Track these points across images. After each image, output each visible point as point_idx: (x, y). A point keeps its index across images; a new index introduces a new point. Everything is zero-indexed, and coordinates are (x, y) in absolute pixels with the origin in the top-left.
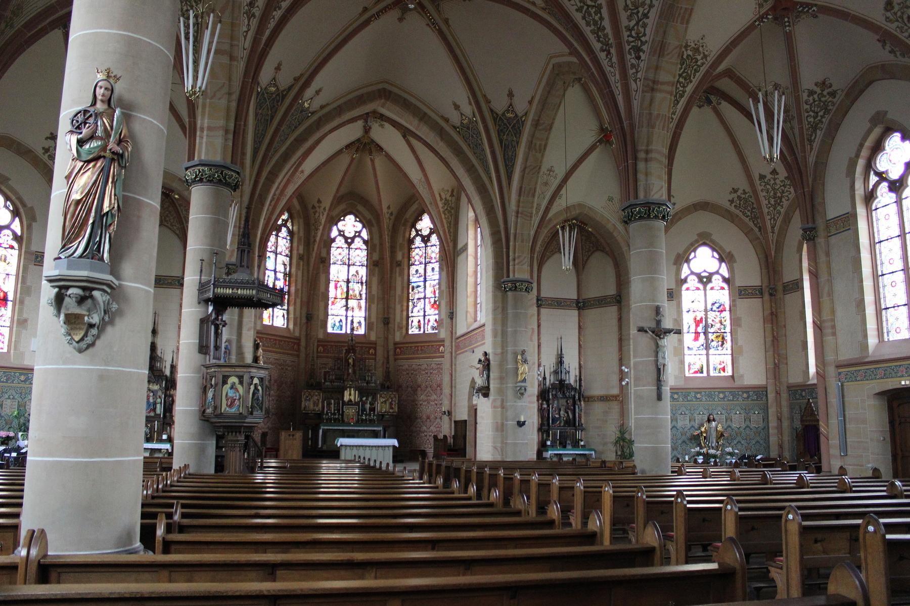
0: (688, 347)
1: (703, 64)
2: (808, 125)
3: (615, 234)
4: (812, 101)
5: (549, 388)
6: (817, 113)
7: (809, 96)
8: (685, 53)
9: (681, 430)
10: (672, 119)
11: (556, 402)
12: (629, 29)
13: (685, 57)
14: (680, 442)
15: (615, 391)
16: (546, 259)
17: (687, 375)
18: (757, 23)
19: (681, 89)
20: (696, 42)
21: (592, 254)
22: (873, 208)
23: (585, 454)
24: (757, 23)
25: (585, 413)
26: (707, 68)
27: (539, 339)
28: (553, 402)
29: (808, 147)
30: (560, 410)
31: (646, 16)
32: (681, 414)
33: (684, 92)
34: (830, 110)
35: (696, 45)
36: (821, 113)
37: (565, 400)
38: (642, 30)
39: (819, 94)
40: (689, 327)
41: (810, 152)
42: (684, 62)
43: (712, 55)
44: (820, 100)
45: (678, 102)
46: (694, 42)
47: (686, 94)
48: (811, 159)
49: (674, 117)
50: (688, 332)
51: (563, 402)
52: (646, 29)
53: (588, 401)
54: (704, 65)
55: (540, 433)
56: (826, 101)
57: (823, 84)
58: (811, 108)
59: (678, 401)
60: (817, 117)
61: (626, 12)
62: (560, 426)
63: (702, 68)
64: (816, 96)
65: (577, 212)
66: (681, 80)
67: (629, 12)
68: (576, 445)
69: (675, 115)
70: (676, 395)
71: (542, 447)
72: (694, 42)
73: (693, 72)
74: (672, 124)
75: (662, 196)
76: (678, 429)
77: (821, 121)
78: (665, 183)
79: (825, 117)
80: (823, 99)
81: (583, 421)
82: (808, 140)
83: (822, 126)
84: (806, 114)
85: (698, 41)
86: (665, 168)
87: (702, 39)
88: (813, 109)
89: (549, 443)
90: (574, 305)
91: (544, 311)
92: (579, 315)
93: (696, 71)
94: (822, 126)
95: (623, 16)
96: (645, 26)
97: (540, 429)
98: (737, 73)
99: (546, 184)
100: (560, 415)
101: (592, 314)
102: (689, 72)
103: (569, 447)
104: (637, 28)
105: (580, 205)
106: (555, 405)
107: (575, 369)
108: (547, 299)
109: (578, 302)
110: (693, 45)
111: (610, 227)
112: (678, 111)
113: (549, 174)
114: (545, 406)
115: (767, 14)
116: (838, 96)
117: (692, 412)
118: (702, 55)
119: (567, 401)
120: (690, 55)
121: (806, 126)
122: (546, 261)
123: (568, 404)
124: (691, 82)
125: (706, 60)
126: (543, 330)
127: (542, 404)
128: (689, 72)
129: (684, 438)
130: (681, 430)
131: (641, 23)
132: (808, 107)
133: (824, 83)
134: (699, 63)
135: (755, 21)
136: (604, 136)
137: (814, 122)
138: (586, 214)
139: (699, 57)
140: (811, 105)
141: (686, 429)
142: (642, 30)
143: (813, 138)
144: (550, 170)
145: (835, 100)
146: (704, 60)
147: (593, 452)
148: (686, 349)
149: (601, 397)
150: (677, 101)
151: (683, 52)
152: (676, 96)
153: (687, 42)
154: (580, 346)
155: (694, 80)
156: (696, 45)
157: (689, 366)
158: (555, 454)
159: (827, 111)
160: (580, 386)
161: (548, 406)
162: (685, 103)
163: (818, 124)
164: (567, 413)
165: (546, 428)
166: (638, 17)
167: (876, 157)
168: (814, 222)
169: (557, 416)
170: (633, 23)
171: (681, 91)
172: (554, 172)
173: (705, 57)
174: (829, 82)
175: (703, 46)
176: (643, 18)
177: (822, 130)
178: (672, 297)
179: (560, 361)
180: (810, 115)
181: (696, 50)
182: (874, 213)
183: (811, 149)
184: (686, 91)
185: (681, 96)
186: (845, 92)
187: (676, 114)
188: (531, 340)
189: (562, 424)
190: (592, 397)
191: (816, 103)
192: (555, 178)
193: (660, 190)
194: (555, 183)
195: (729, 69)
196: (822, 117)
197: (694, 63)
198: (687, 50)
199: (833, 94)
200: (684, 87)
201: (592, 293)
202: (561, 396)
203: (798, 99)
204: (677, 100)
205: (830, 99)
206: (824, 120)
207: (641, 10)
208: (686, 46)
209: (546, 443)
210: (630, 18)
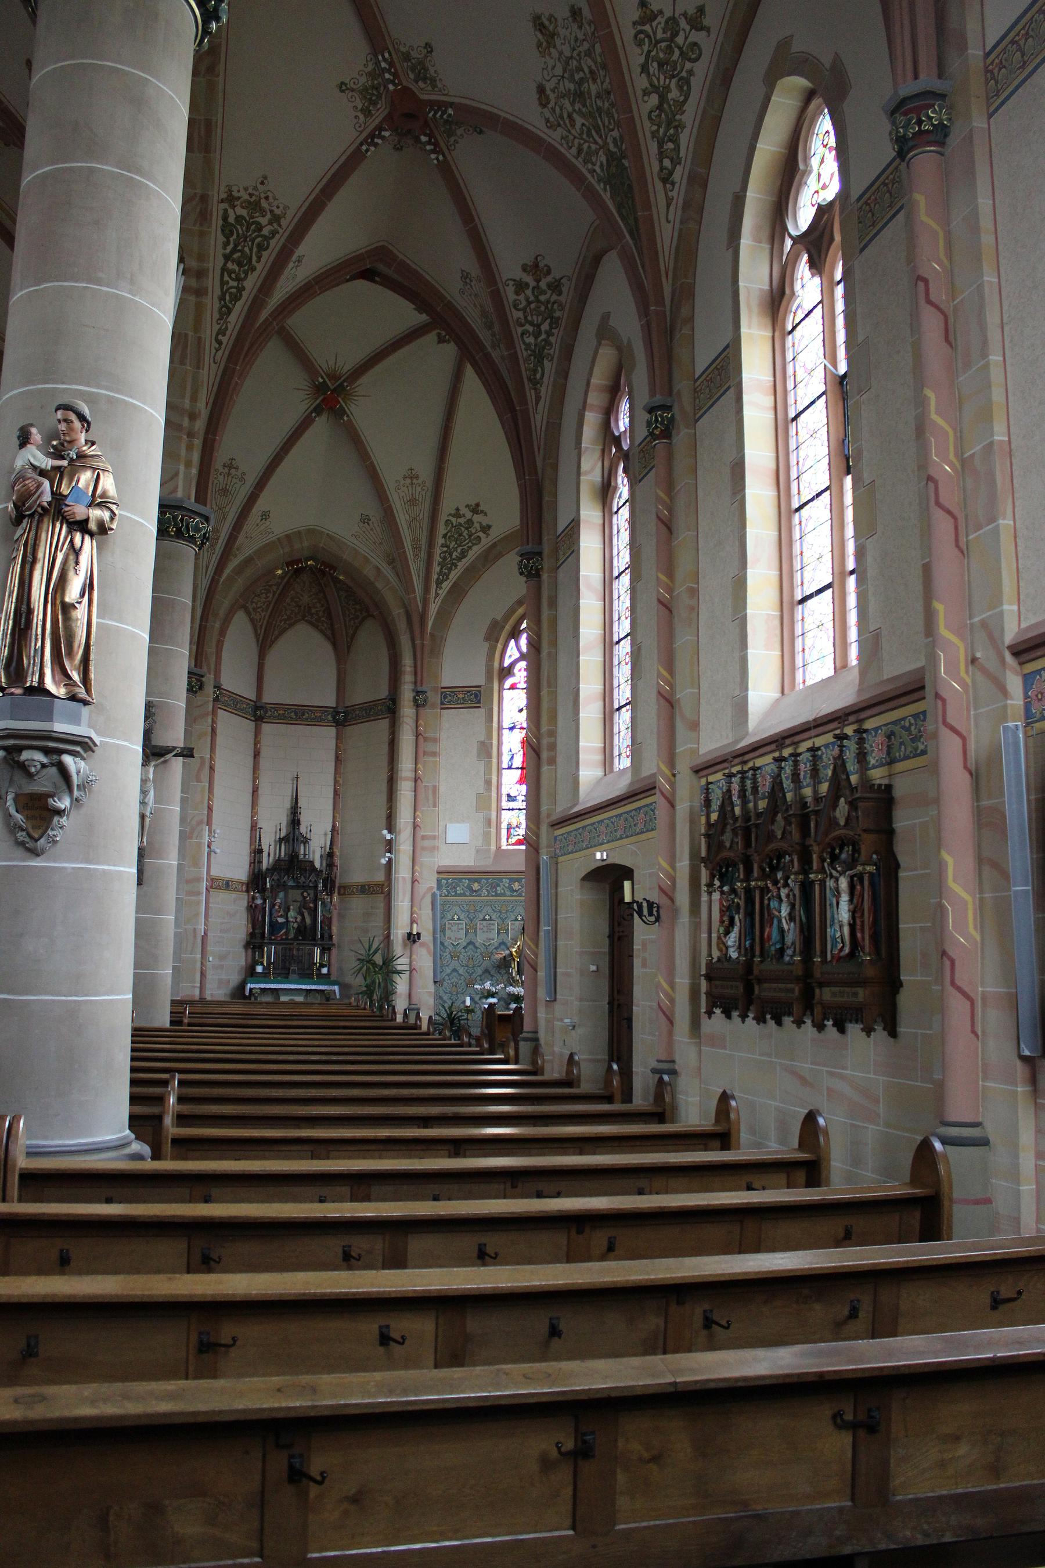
0: (509, 795)
1: (274, 233)
2: (526, 350)
3: (379, 585)
4: (524, 303)
5: (267, 869)
6: (539, 326)
7: (517, 293)
8: (230, 211)
9: (483, 949)
10: (220, 343)
11: (281, 895)
13: (231, 219)
14: (479, 971)
15: (380, 877)
16: (276, 632)
17: (504, 847)
18: (364, 148)
19: (235, 284)
20: (250, 191)
21: (361, 623)
22: (615, 509)
23: (322, 991)
24: (364, 148)
25: (339, 914)
26: (283, 240)
27: (255, 778)
29: (530, 394)
30: (289, 910)
32: (484, 919)
33: (241, 290)
34: (559, 318)
35: (251, 195)
36: (545, 327)
37: (299, 891)
39: (534, 288)
40: (512, 757)
41: (537, 404)
42: (232, 234)
43: (289, 216)
44: (538, 301)
45: (230, 311)
46: (246, 189)
47: (245, 294)
48: (538, 417)
49: (224, 339)
50: (510, 768)
51: (295, 894)
53: (344, 894)
54: (277, 236)
55: (250, 951)
56: (548, 302)
57: (535, 268)
58: (526, 317)
59: (480, 896)
60: (540, 333)
63: (273, 242)
64: (529, 292)
65: (306, 544)
66: (230, 265)
68: (307, 973)
69: (224, 335)
70: (476, 884)
71: (250, 973)
72: (246, 189)
73: (255, 249)
74: (220, 353)
75: (175, 490)
76: (476, 948)
77: (547, 342)
78: (188, 464)
79: (553, 335)
80: (542, 298)
81: (335, 929)
82: (529, 379)
83: (551, 352)
84: (520, 330)
85: (255, 188)
86: (191, 435)
87: (262, 183)
88: (529, 318)
89: (259, 969)
90: (330, 718)
91: (266, 728)
92: (339, 737)
93: (261, 248)
94: (551, 352)
97: (247, 946)
98: (398, 254)
99: (225, 491)
100: (287, 918)
101: (356, 732)
102: (247, 249)
103: (292, 976)
105: (311, 532)
106: (279, 901)
107: (326, 834)
108: (276, 706)
109: (335, 711)
110: (246, 197)
111: (369, 572)
112: (230, 327)
113: (229, 474)
114: (259, 902)
115: (380, 128)
116: (564, 289)
117: (503, 916)
118: (269, 216)
119: (302, 894)
120: (243, 217)
121: (523, 353)
122: (277, 638)
124: (253, 269)
125: (280, 226)
126: (263, 762)
127: (254, 898)
128: (247, 249)
129: (487, 964)
130: (483, 949)
132: (520, 314)
133: (536, 265)
134: (265, 232)
135: (361, 144)
136: (323, 401)
137: (536, 345)
138: (323, 549)
139: (264, 221)
140: (524, 310)
141: (491, 949)
143: (538, 376)
144: (230, 466)
145: (562, 299)
146: (275, 225)
147: (336, 988)
148: (504, 798)
149: (361, 886)
150: (228, 308)
151: (226, 211)
152: (222, 298)
153: (230, 191)
154: (336, 793)
155: (259, 267)
156: (251, 195)
157: (508, 830)
158: (261, 989)
159: (555, 322)
160: (331, 865)
161: (264, 902)
162: (244, 314)
163: (544, 348)
165: (258, 941)
167: (618, 407)
168: (540, 543)
169: (281, 920)
171: (232, 287)
172: (237, 469)
173: (276, 219)
174: (545, 262)
175: (267, 198)
177: (552, 360)
178: (479, 702)
179: (295, 822)
180: (528, 331)
181: (254, 206)
182: (615, 517)
183: (538, 399)
184: (244, 289)
185: (236, 298)
186: (574, 281)
187: (228, 333)
188: (199, 780)
189: (291, 936)
190: (350, 886)
191: (533, 306)
192: (242, 479)
193: (172, 478)
194: (243, 492)
195: (383, 247)
196: (549, 334)
197: (255, 231)
198: (233, 207)
199: (556, 287)
200: (238, 279)
201: (361, 694)
202: (291, 883)
203: (497, 296)
204: (226, 306)
205: (554, 297)
206: (552, 339)
208: (231, 199)
209: (255, 969)
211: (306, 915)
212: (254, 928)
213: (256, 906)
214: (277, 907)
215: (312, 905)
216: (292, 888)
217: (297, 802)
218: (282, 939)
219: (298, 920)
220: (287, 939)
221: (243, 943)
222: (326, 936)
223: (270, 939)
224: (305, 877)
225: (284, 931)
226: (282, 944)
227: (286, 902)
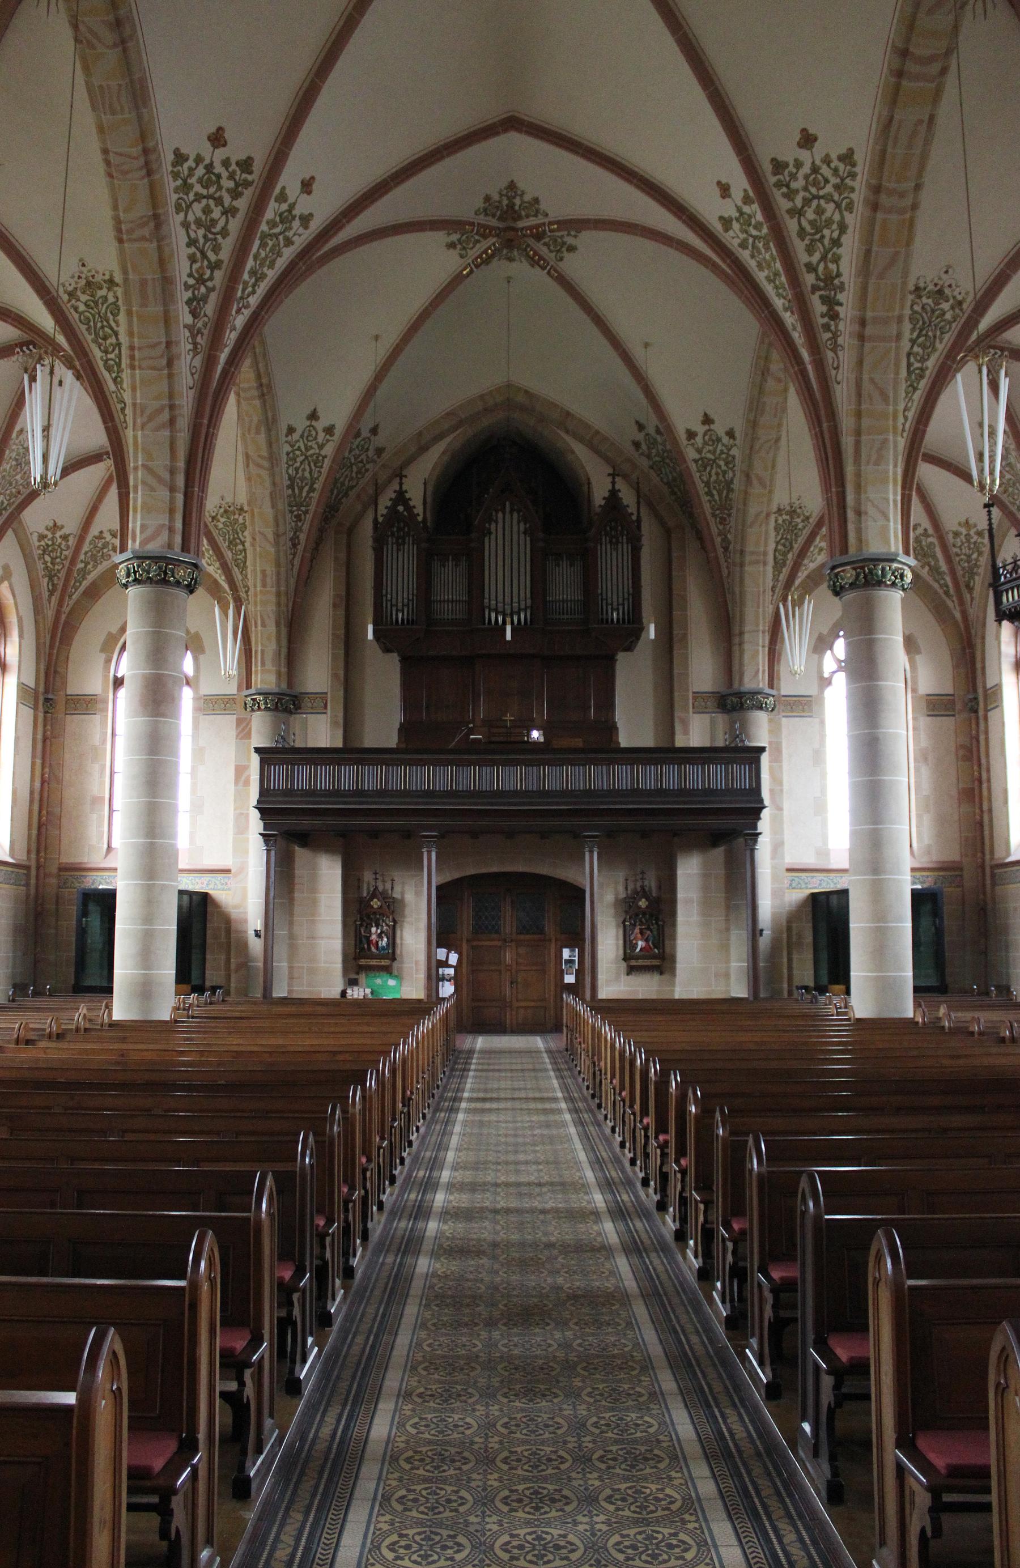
12: (811, 268)
31: (836, 243)
38: (833, 267)
52: (840, 263)
61: (803, 240)
67: (807, 242)
95: (799, 247)
96: (836, 260)
104: (826, 264)
131: (830, 256)
142: (833, 267)
166: (823, 246)
170: (817, 256)
176: (831, 249)
207: (826, 232)
210: (810, 250)
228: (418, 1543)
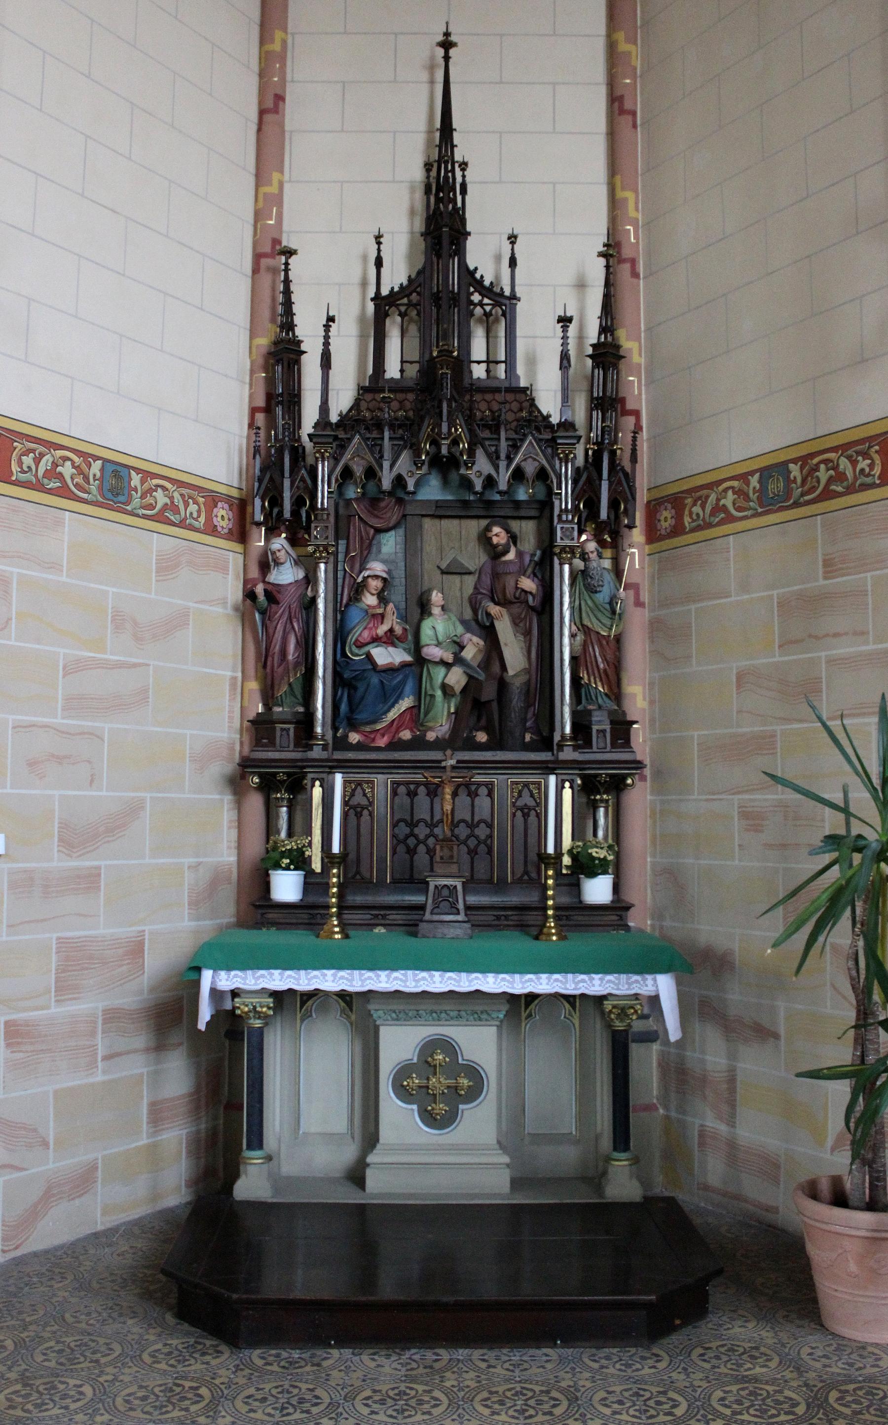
25: (656, 627)
28: (367, 549)
30: (424, 608)
37: (473, 527)
53: (677, 530)
55: (255, 802)
62: (418, 743)
100: (417, 649)
106: (377, 567)
119: (484, 539)
123: (496, 553)
149: (766, 473)
161: (310, 579)
164: (489, 633)
169: (384, 656)
190: (699, 493)
209: (266, 887)
211: (504, 628)
212: (268, 696)
213: (273, 595)
214: (370, 600)
215: (528, 584)
216: (440, 511)
217: (447, 129)
218: (395, 745)
219: (469, 653)
220: (418, 743)
221: (227, 766)
222: (600, 723)
223: (341, 744)
224: (494, 458)
225: (406, 703)
226: (398, 765)
227: (411, 576)
228: (291, 1404)
